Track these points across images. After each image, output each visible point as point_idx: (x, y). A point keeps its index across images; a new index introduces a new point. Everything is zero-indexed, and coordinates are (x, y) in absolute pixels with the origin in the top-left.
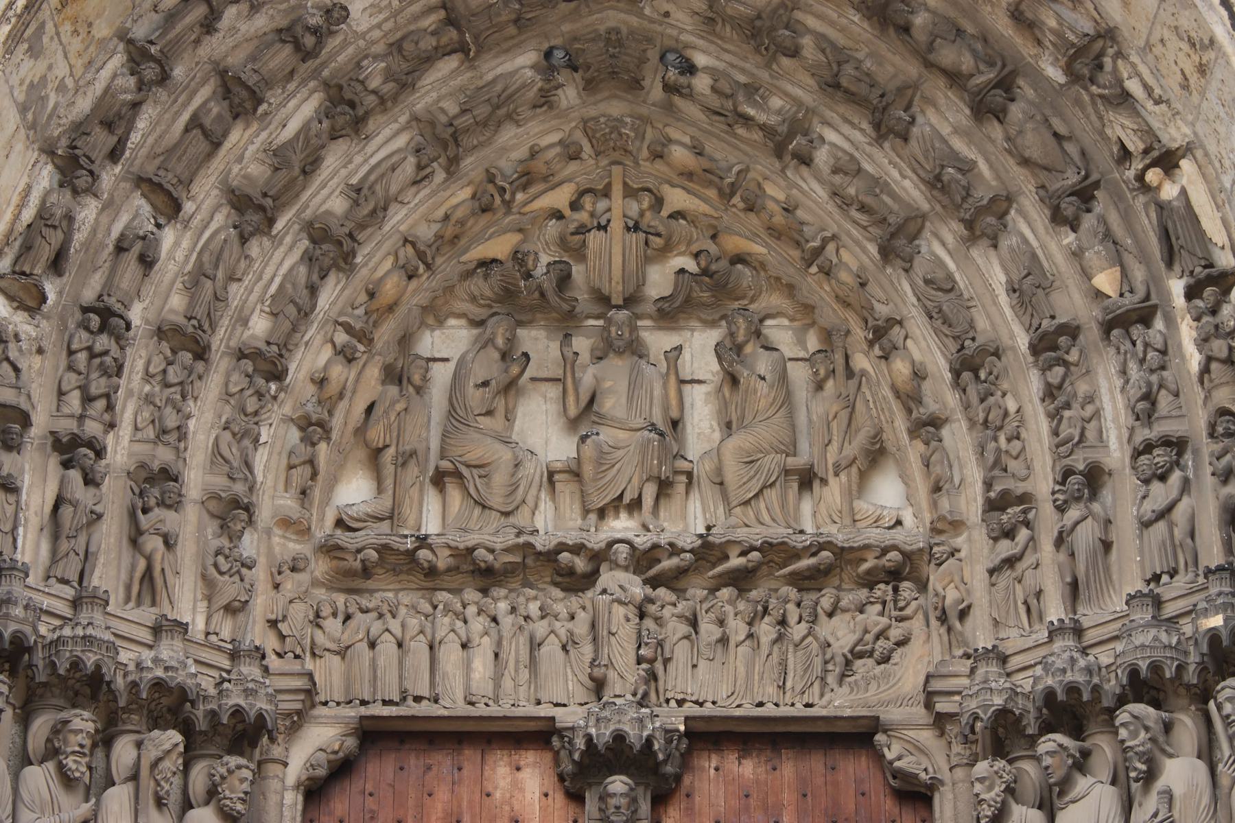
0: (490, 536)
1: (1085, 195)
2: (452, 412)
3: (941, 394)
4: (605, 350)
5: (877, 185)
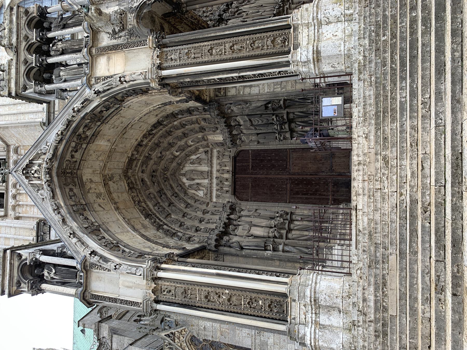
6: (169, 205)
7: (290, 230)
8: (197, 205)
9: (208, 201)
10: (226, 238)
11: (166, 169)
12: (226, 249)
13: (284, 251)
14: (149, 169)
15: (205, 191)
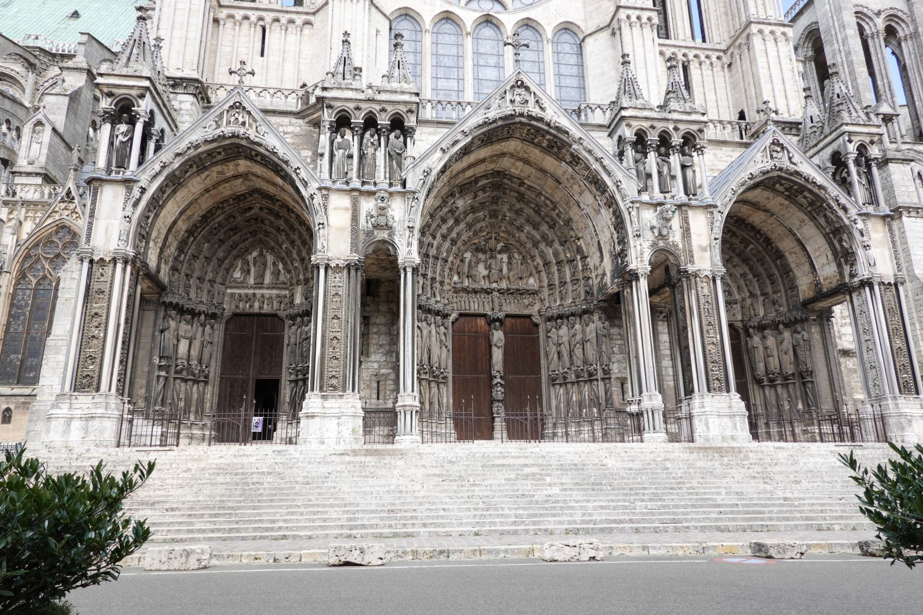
0: (476, 286)
1: (565, 242)
2: (469, 266)
3: (541, 268)
4: (491, 258)
5: (533, 236)
6: (220, 240)
7: (185, 381)
8: (222, 272)
9: (227, 283)
10: (173, 313)
11: (267, 234)
12: (162, 314)
13: (159, 377)
14: (264, 214)
15: (239, 280)
